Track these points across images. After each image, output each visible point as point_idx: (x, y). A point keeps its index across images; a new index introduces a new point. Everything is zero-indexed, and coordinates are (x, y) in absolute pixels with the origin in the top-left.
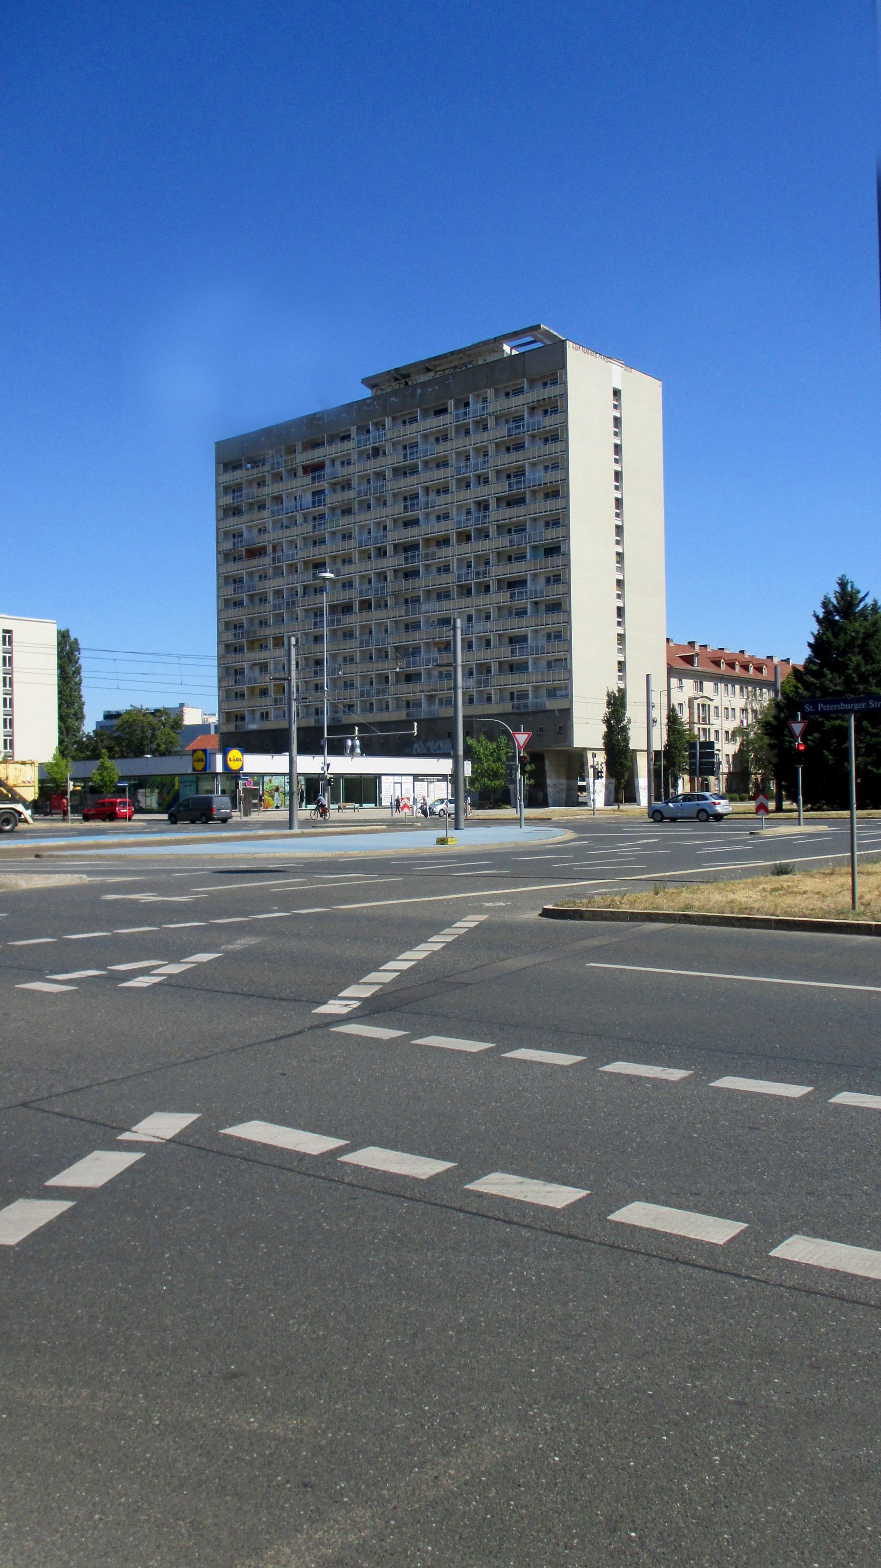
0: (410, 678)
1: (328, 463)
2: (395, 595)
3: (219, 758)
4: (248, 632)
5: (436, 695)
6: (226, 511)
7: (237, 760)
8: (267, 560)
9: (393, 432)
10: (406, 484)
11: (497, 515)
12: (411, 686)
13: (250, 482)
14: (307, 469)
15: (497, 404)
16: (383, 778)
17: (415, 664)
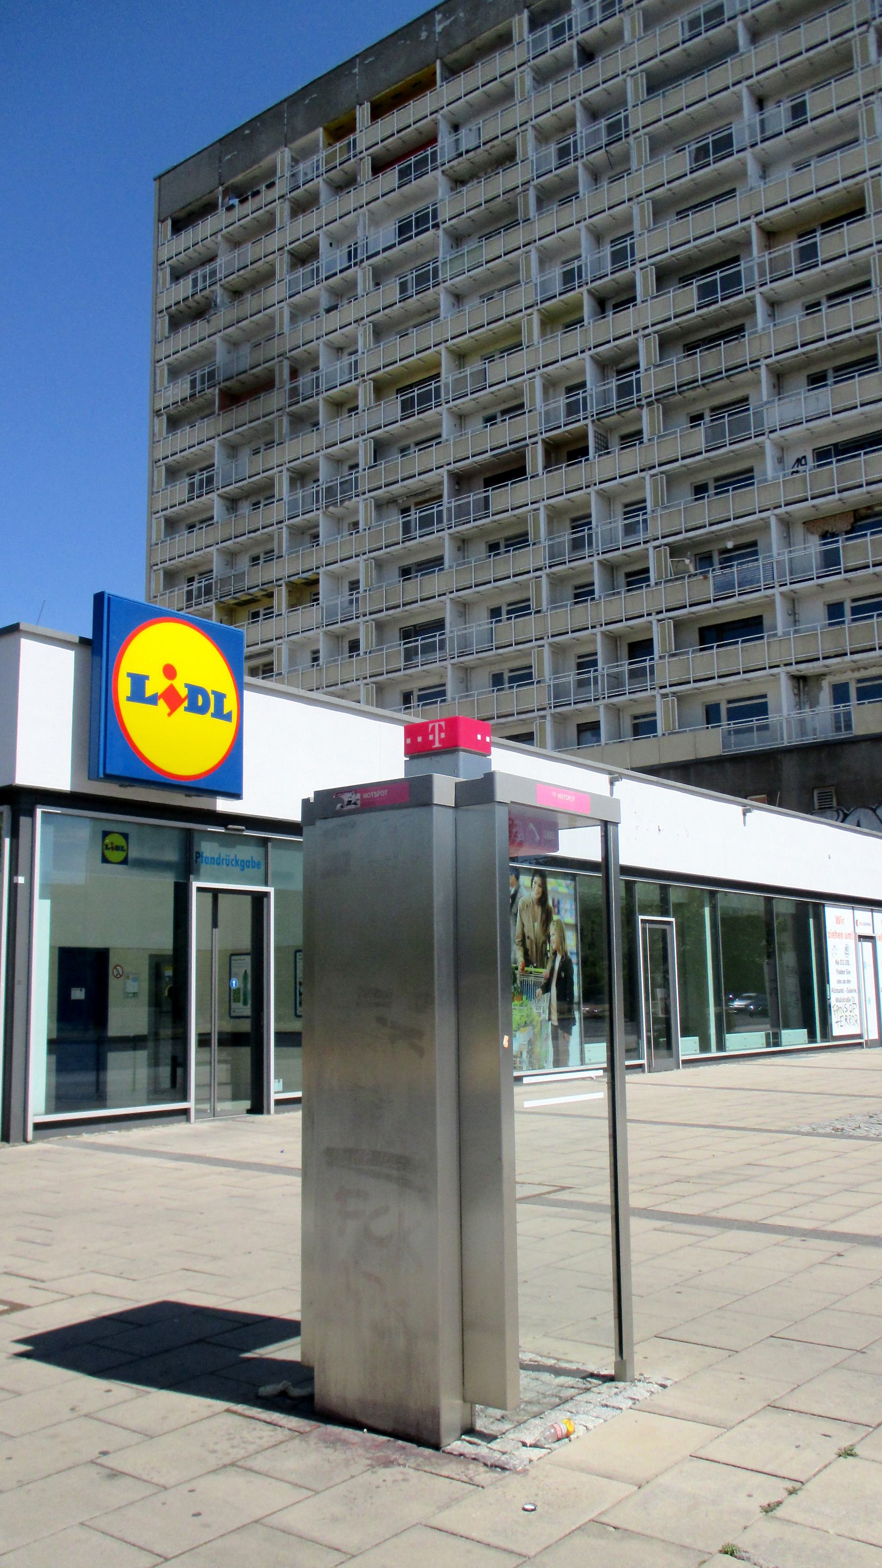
3: (47, 677)
4: (224, 581)
5: (821, 676)
6: (171, 525)
7: (197, 700)
8: (276, 399)
12: (738, 653)
16: (832, 914)
17: (748, 584)
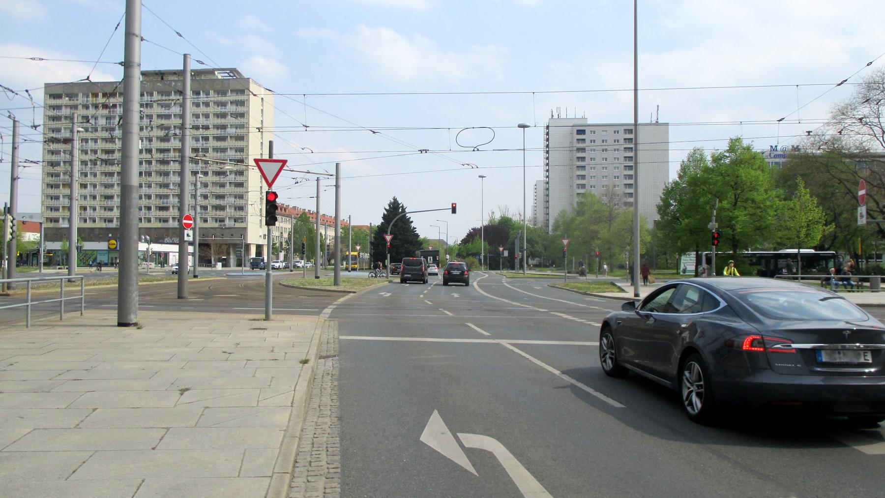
0: (162, 209)
2: (157, 172)
11: (212, 143)
13: (66, 106)
15: (213, 97)
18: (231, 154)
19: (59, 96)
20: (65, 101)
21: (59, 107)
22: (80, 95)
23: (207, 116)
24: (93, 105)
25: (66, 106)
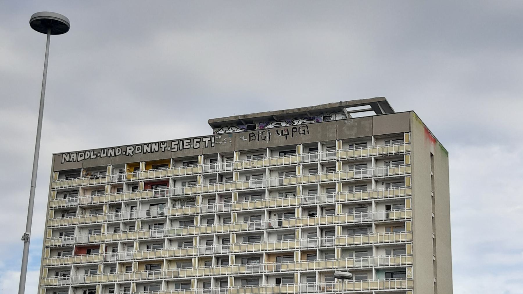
1: (171, 182)
9: (239, 163)
10: (250, 205)
11: (341, 239)
13: (85, 190)
14: (150, 185)
15: (343, 152)
18: (379, 259)
19: (72, 174)
20: (82, 181)
21: (74, 192)
22: (110, 169)
23: (330, 187)
24: (128, 185)
25: (85, 190)
